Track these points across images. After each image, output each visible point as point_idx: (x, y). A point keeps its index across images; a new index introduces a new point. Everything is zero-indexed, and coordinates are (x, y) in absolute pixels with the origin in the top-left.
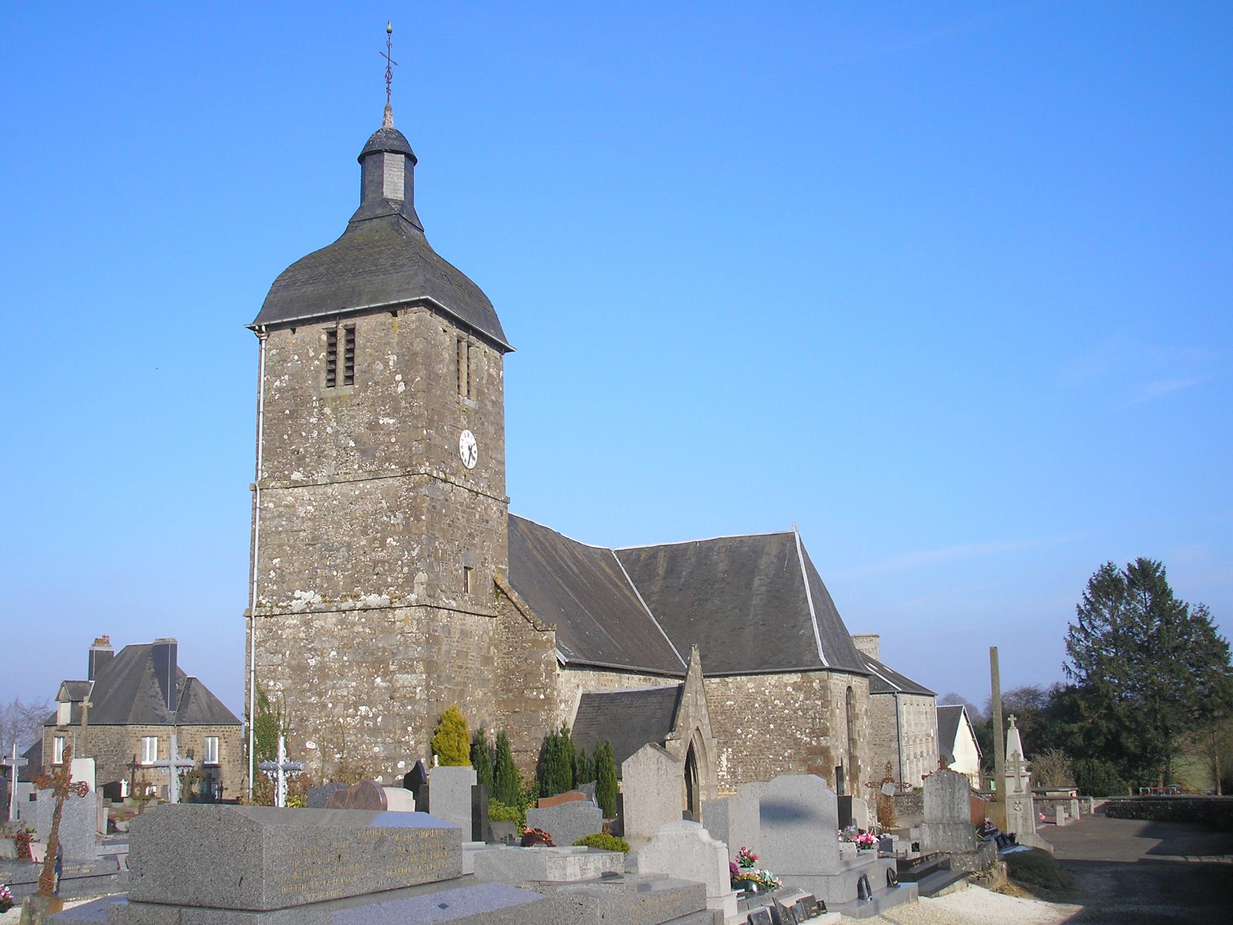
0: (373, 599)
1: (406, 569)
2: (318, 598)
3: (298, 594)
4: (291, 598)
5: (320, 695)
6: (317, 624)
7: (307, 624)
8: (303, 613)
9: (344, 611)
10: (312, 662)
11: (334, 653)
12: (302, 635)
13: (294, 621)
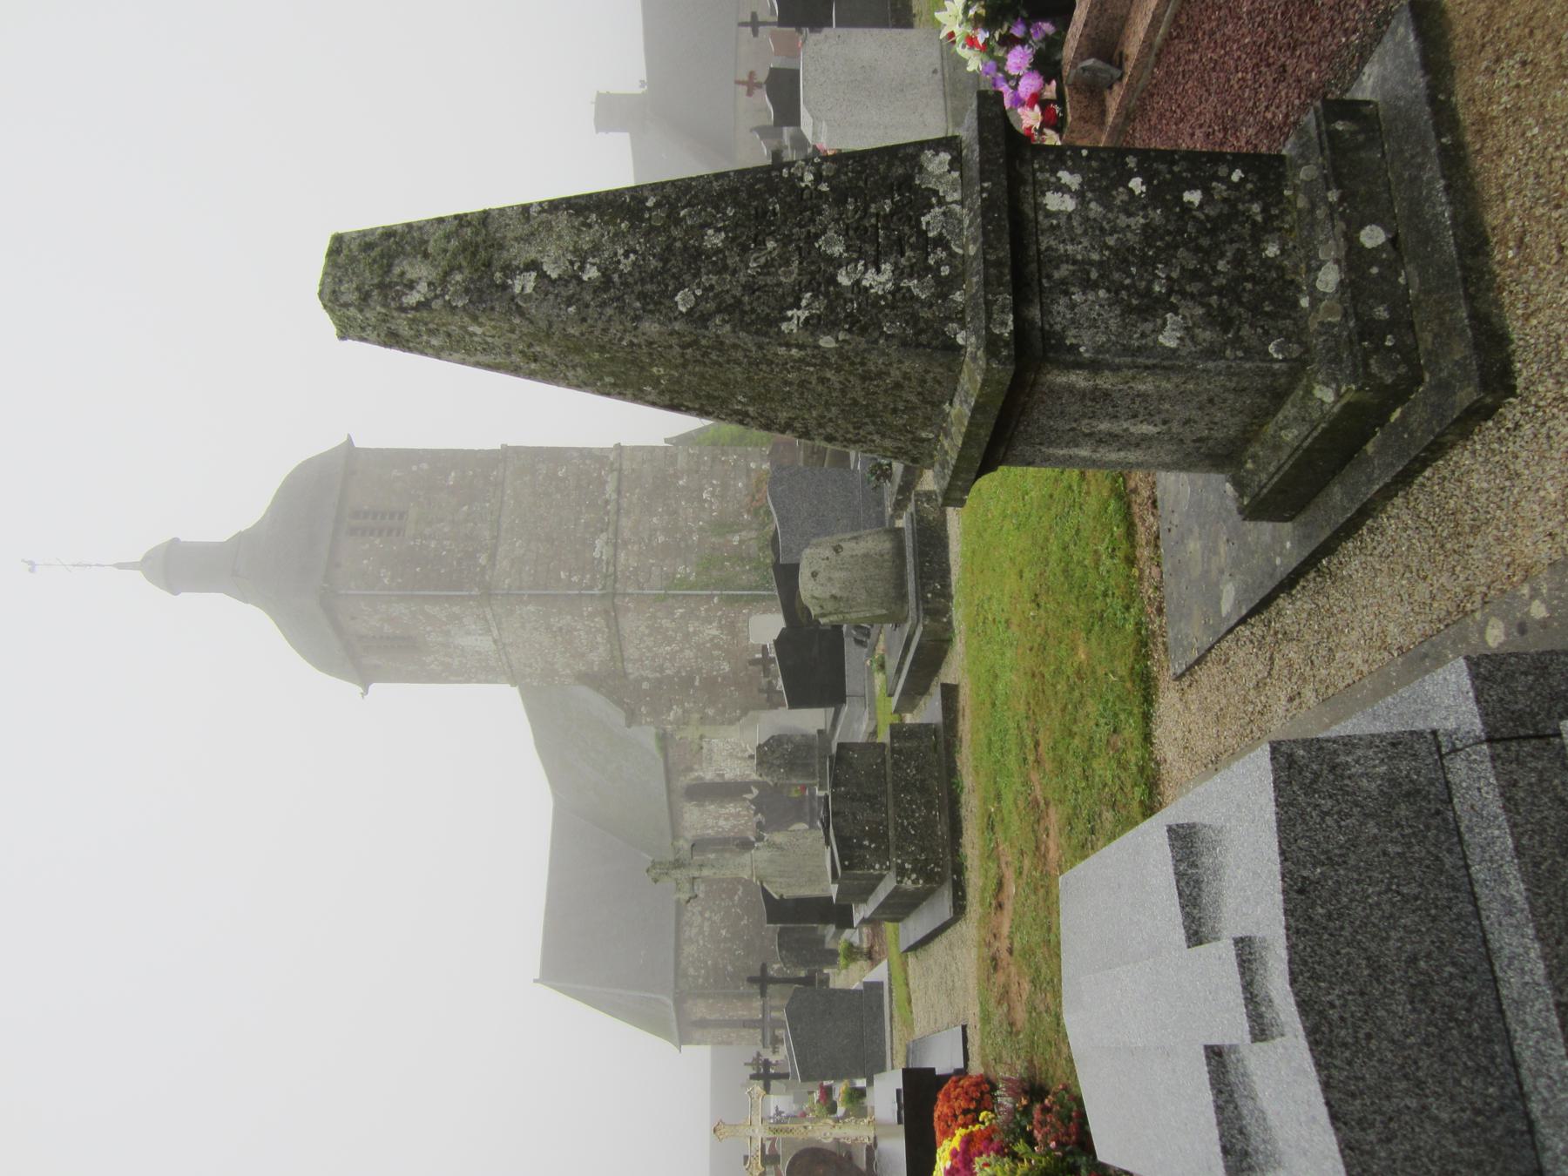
0: (610, 488)
1: (588, 462)
2: (604, 536)
3: (596, 554)
4: (600, 559)
5: (691, 532)
6: (626, 534)
7: (625, 543)
8: (615, 546)
9: (619, 510)
10: (661, 539)
11: (655, 520)
12: (636, 548)
13: (622, 556)
